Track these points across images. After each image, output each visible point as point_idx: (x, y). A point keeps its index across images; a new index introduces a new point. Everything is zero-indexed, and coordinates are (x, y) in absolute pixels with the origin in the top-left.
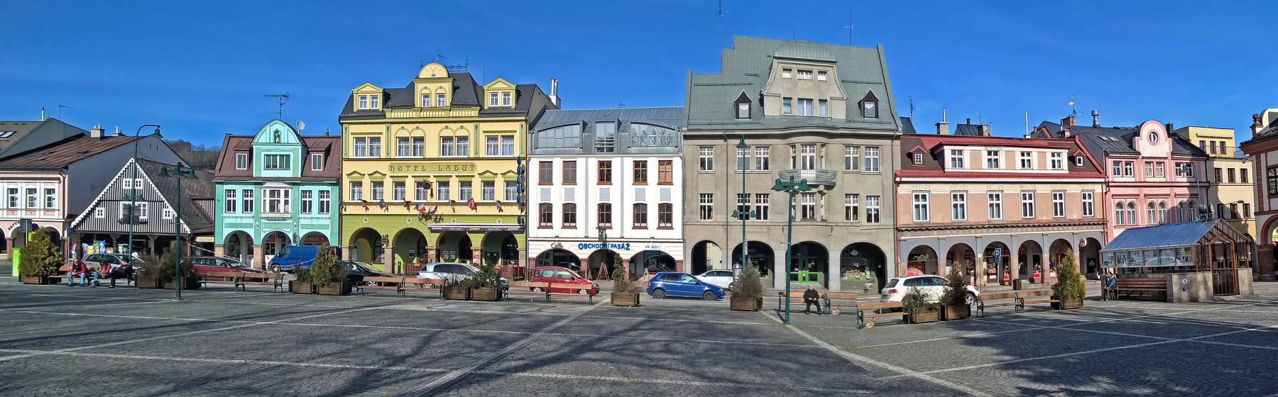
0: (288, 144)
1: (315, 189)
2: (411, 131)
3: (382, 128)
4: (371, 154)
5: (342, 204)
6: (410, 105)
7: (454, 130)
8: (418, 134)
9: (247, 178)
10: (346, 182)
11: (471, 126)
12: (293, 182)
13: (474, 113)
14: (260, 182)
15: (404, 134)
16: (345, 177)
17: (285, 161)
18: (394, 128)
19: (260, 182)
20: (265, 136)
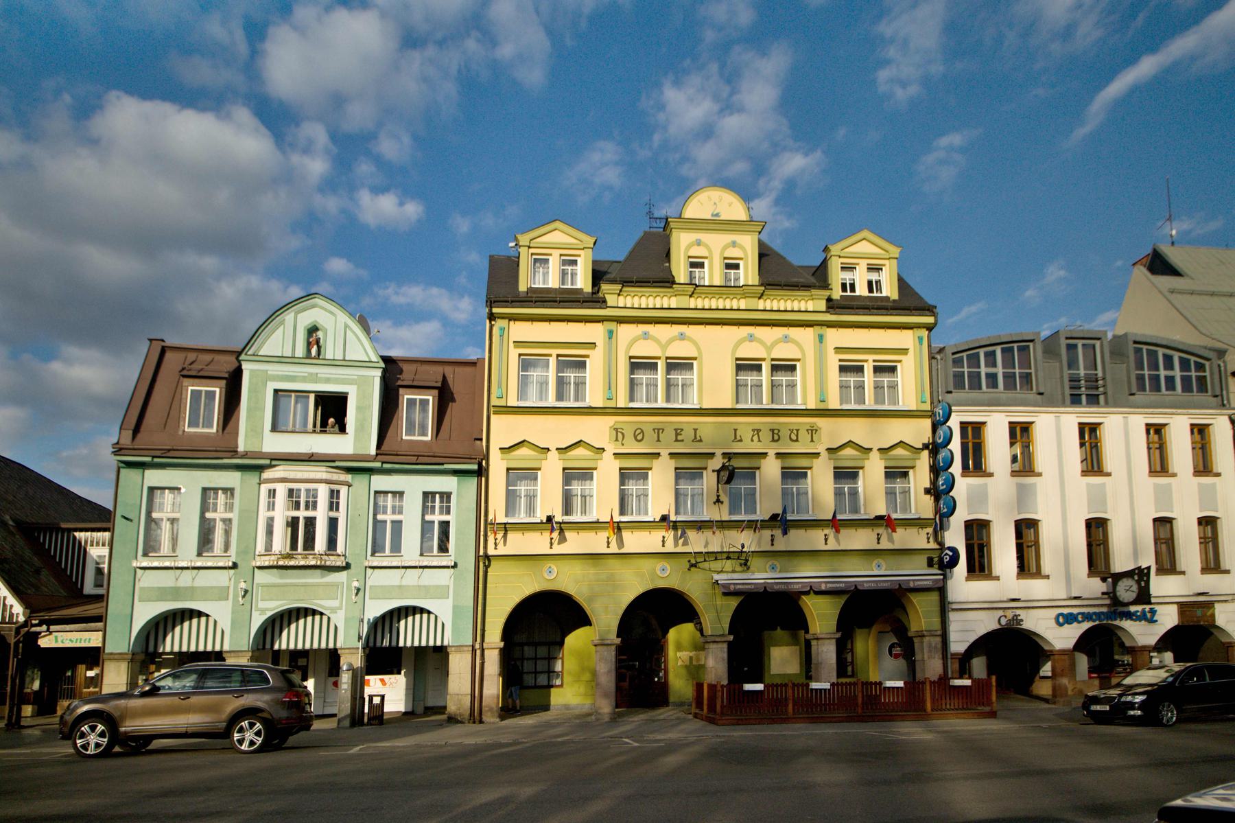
0: (346, 363)
1: (414, 486)
2: (660, 342)
3: (595, 332)
4: (560, 396)
5: (483, 525)
6: (667, 281)
7: (767, 344)
8: (679, 350)
9: (220, 453)
10: (497, 467)
11: (806, 336)
12: (356, 468)
13: (812, 303)
14: (255, 466)
15: (644, 349)
16: (495, 455)
17: (332, 409)
18: (626, 332)
19: (255, 466)
20: (283, 339)
